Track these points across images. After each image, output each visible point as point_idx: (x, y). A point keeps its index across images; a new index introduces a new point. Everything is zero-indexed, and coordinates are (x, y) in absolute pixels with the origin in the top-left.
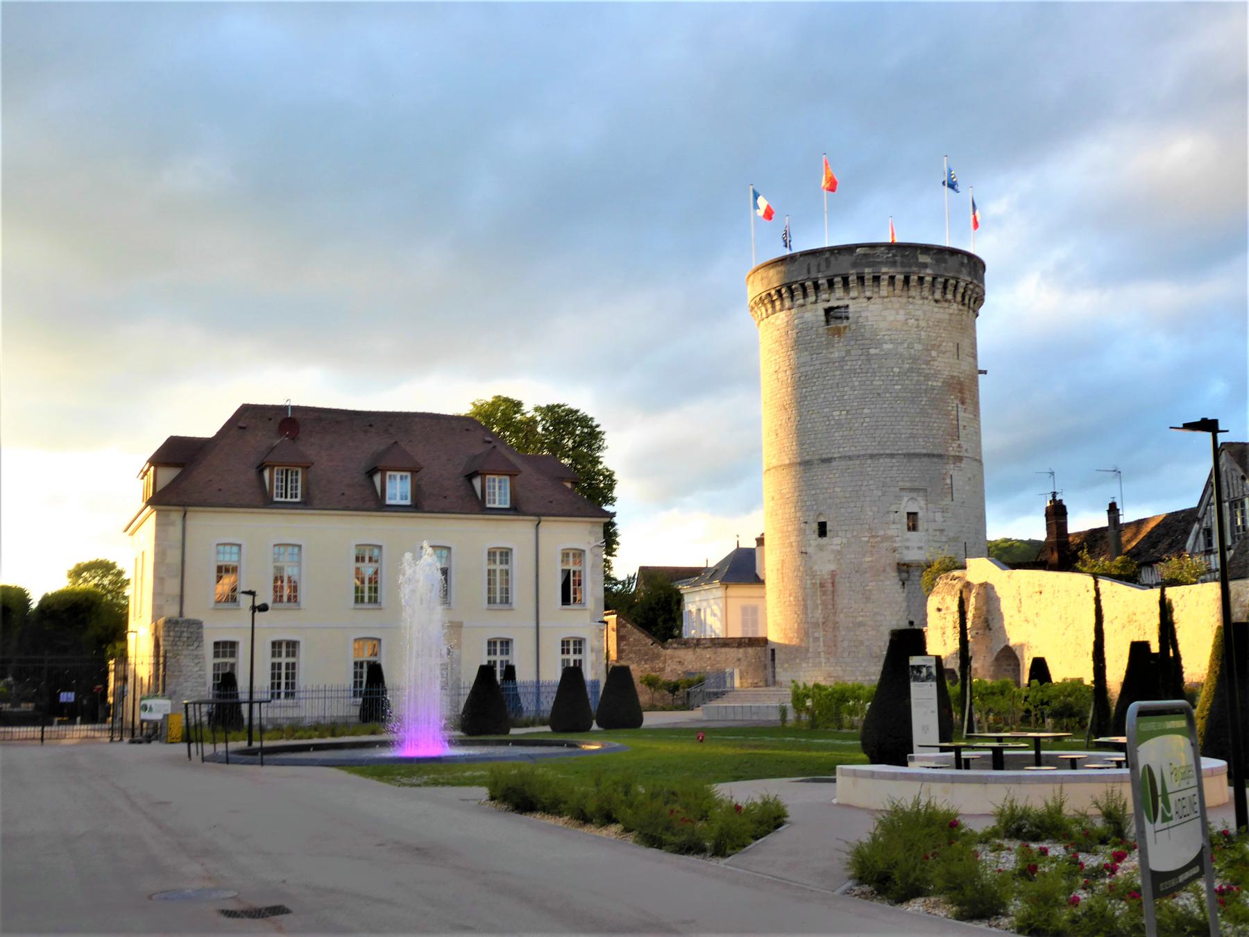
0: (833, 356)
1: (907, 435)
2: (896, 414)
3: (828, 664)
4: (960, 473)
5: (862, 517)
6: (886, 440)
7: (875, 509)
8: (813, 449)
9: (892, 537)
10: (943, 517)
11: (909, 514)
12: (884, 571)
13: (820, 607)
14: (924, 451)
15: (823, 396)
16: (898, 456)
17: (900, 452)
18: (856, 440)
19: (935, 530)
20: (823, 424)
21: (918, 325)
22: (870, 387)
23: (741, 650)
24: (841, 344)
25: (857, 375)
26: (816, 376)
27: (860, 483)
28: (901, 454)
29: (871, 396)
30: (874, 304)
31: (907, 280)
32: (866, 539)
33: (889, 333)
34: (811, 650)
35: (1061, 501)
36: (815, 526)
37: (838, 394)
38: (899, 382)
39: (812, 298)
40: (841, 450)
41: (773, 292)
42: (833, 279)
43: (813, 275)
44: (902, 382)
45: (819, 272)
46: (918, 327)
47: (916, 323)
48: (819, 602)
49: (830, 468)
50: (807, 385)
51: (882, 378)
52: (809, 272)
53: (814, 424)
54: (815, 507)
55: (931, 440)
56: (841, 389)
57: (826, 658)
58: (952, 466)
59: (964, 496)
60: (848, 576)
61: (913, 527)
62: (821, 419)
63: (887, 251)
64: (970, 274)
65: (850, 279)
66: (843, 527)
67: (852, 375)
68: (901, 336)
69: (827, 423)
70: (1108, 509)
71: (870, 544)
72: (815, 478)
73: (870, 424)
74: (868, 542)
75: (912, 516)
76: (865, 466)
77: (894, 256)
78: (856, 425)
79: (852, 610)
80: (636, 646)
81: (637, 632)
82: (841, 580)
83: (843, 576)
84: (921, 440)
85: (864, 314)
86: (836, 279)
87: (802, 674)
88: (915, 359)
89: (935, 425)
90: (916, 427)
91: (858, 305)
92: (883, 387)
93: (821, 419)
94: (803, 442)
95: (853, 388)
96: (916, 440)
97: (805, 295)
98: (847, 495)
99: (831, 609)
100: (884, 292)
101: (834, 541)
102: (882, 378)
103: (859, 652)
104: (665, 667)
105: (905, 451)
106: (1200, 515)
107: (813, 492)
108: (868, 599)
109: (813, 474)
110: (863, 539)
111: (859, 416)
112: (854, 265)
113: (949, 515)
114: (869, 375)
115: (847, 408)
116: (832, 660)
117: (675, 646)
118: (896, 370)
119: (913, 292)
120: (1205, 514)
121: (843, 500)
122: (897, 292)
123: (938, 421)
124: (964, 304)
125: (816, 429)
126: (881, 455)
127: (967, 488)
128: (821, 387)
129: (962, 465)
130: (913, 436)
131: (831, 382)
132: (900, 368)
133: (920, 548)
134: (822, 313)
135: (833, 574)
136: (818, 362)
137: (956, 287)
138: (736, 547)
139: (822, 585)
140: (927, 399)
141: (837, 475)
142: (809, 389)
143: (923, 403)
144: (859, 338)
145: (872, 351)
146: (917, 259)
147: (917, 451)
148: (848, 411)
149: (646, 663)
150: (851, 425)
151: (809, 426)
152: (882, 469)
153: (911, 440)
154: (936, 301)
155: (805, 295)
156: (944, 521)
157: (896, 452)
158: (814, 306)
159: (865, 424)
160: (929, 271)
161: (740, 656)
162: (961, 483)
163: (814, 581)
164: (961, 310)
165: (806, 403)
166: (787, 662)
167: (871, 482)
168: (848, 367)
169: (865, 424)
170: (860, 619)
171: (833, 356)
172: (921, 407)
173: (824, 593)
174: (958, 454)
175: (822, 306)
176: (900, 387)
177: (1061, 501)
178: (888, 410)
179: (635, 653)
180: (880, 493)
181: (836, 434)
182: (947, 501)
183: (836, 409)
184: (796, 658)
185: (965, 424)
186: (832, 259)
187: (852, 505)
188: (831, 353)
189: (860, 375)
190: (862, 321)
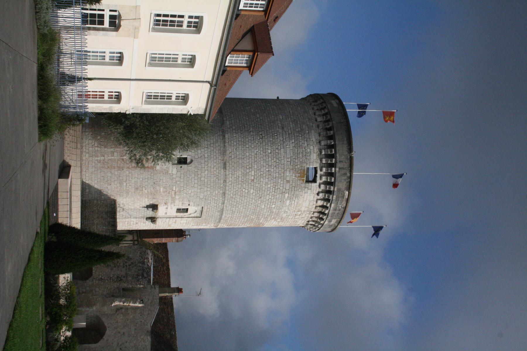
3: (96, 162)
5: (188, 187)
6: (233, 200)
7: (192, 194)
8: (233, 157)
9: (174, 202)
11: (187, 209)
15: (265, 165)
17: (225, 207)
22: (266, 193)
25: (274, 186)
28: (223, 208)
29: (260, 193)
30: (314, 197)
32: (174, 189)
34: (106, 149)
37: (264, 175)
40: (230, 176)
42: (334, 177)
43: (339, 165)
45: (340, 169)
50: (272, 153)
51: (270, 199)
52: (340, 162)
56: (267, 177)
61: (179, 210)
63: (343, 206)
67: (274, 184)
69: (248, 167)
70: (180, 287)
71: (171, 191)
72: (215, 157)
74: (173, 190)
76: (219, 190)
77: (339, 210)
78: (244, 185)
79: (131, 180)
83: (152, 175)
85: (309, 191)
92: (265, 200)
94: (238, 148)
98: (202, 179)
102: (270, 199)
105: (225, 209)
107: (206, 156)
108: (137, 189)
110: (174, 187)
111: (250, 187)
112: (339, 190)
114: (273, 193)
115: (255, 181)
118: (273, 206)
125: (245, 159)
126: (225, 198)
128: (270, 164)
132: (274, 208)
136: (285, 162)
141: (215, 172)
143: (252, 217)
144: (296, 189)
146: (333, 182)
147: (224, 214)
148: (253, 180)
151: (247, 154)
152: (216, 198)
154: (308, 221)
159: (244, 190)
165: (262, 153)
167: (209, 193)
168: (280, 181)
169: (244, 190)
170: (125, 184)
181: (240, 173)
183: (256, 174)
187: (196, 181)
188: (290, 172)
189: (274, 189)
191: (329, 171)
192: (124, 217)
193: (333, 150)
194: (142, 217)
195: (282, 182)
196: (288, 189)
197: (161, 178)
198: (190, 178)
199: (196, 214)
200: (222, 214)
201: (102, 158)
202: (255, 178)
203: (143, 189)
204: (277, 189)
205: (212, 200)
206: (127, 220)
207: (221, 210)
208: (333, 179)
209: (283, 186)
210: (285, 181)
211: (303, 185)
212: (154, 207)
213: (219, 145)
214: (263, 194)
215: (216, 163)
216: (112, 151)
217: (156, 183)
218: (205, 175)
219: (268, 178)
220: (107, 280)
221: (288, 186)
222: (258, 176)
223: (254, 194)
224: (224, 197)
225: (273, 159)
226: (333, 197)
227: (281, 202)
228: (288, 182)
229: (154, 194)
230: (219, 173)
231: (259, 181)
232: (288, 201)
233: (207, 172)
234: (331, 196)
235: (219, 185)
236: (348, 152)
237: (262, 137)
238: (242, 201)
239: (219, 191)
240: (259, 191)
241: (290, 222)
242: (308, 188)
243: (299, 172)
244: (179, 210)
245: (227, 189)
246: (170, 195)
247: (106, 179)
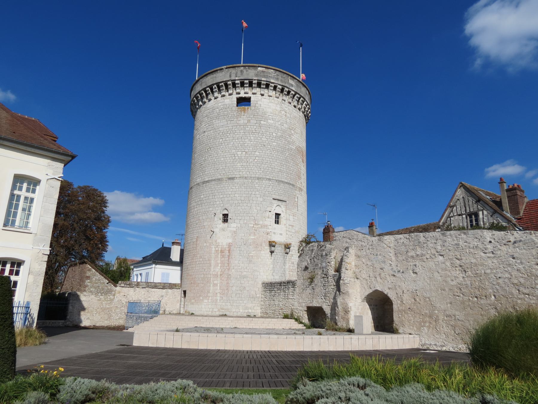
0: (240, 122)
1: (278, 170)
2: (273, 158)
5: (251, 212)
6: (267, 171)
7: (259, 208)
8: (224, 172)
9: (267, 226)
10: (293, 219)
12: (261, 245)
13: (219, 265)
14: (286, 181)
16: (273, 181)
18: (250, 169)
19: (289, 225)
20: (231, 158)
21: (286, 115)
22: (260, 141)
23: (164, 290)
24: (245, 116)
25: (253, 133)
26: (229, 132)
28: (275, 180)
29: (260, 145)
30: (265, 99)
32: (253, 225)
33: (272, 115)
37: (241, 143)
38: (276, 141)
40: (241, 173)
43: (233, 78)
44: (277, 142)
45: (236, 76)
47: (285, 114)
48: (219, 262)
49: (233, 183)
50: (223, 138)
51: (266, 137)
52: (230, 76)
53: (225, 159)
54: (222, 205)
55: (290, 176)
56: (243, 140)
57: (221, 297)
60: (239, 246)
61: (277, 222)
62: (230, 156)
66: (238, 218)
67: (250, 133)
68: (278, 118)
69: (234, 158)
71: (254, 229)
72: (223, 188)
73: (259, 160)
75: (277, 215)
76: (254, 183)
77: (278, 75)
78: (251, 160)
79: (240, 267)
80: (96, 283)
81: (99, 274)
83: (236, 246)
85: (259, 103)
87: (203, 307)
89: (292, 168)
90: (282, 167)
91: (256, 98)
92: (267, 142)
93: (230, 156)
94: (217, 168)
95: (250, 140)
96: (282, 173)
98: (243, 199)
99: (226, 266)
101: (232, 225)
102: (266, 137)
103: (242, 294)
104: (114, 298)
105: (276, 179)
107: (222, 196)
108: (250, 261)
112: (257, 75)
113: (296, 218)
116: (225, 298)
117: (123, 285)
118: (274, 134)
121: (240, 202)
125: (226, 161)
130: (280, 171)
133: (281, 234)
135: (230, 245)
136: (231, 125)
138: (161, 246)
139: (222, 252)
140: (288, 154)
141: (237, 187)
143: (287, 155)
145: (262, 122)
147: (283, 180)
149: (102, 295)
151: (222, 159)
152: (264, 186)
153: (280, 173)
156: (294, 221)
157: (272, 178)
161: (163, 294)
163: (217, 249)
165: (222, 147)
166: (194, 299)
167: (257, 193)
169: (256, 160)
170: (245, 273)
171: (240, 122)
172: (286, 157)
173: (223, 256)
175: (235, 97)
176: (276, 144)
178: (269, 155)
179: (95, 288)
180: (262, 200)
181: (239, 164)
182: (295, 211)
183: (240, 150)
184: (200, 296)
186: (245, 71)
187: (245, 205)
189: (255, 134)
190: (258, 106)
191: (239, 85)
192: (282, 275)
193: (220, 84)
194: (284, 258)
195: (249, 127)
196: (256, 121)
198: (241, 210)
199: (283, 206)
200: (283, 182)
201: (218, 295)
202: (244, 150)
203: (251, 256)
204: (256, 131)
205: (266, 190)
206: (287, 272)
207: (277, 182)
208: (246, 81)
209: (253, 126)
210: (248, 124)
211: (253, 108)
212: (272, 244)
213: (213, 185)
214: (261, 143)
215: (228, 187)
216: (213, 286)
217: (245, 243)
218: (239, 196)
219: (245, 139)
220: (325, 290)
221: (253, 121)
222: (242, 148)
223: (260, 151)
224: (262, 179)
225: (228, 136)
226: (264, 81)
227: (269, 128)
228: (249, 121)
229: (257, 245)
230: (237, 184)
231: (247, 147)
232: (269, 121)
233: (236, 195)
234: (263, 82)
235: (250, 183)
236: (222, 72)
237: (209, 148)
238: (267, 163)
239: (256, 183)
240: (257, 147)
241: (296, 122)
242: (255, 104)
243: (240, 112)
244: (277, 222)
245: (254, 176)
246: (258, 229)
247: (239, 292)
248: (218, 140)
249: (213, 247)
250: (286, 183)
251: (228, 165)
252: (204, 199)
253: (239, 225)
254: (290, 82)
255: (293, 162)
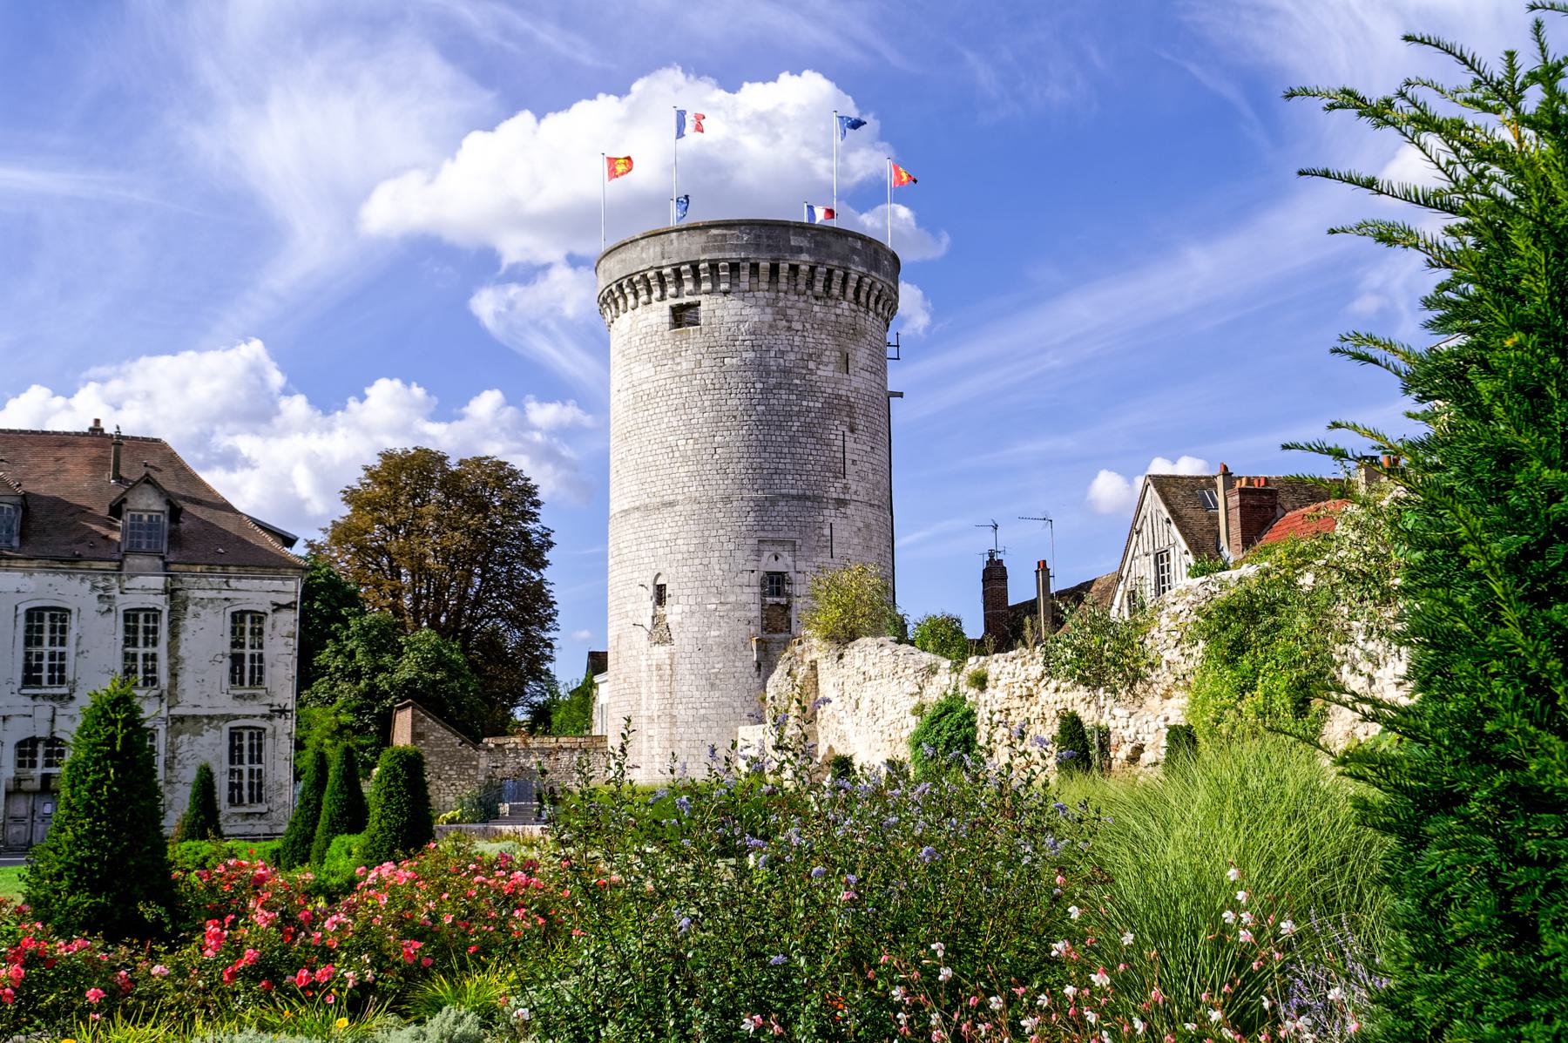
4: (845, 521)
8: (654, 490)
14: (794, 492)
15: (666, 420)
22: (724, 408)
26: (660, 394)
27: (706, 533)
29: (724, 419)
31: (774, 270)
35: (1000, 562)
36: (651, 588)
39: (657, 293)
41: (614, 287)
46: (789, 328)
48: (654, 689)
56: (688, 411)
58: (833, 512)
59: (850, 552)
64: (864, 264)
65: (702, 266)
74: (716, 610)
80: (439, 746)
82: (682, 661)
84: (788, 477)
86: (683, 268)
88: (786, 372)
97: (650, 292)
100: (745, 285)
106: (1124, 574)
107: (652, 545)
109: (652, 522)
114: (723, 391)
115: (696, 435)
118: (759, 385)
119: (783, 285)
120: (1129, 571)
122: (764, 286)
123: (814, 452)
124: (858, 303)
127: (856, 541)
128: (664, 409)
129: (848, 512)
131: (676, 402)
134: (667, 312)
137: (845, 280)
142: (651, 412)
143: (794, 429)
150: (699, 457)
151: (651, 459)
154: (817, 298)
155: (650, 292)
158: (660, 304)
159: (716, 457)
160: (805, 257)
162: (846, 534)
164: (854, 311)
167: (721, 532)
169: (716, 457)
170: (702, 711)
172: (791, 433)
174: (842, 496)
177: (1000, 562)
182: (823, 558)
185: (856, 457)
195: (698, 377)
197: (690, 636)
201: (657, 759)
208: (683, 268)
248: (641, 414)
249: (643, 657)
250: (793, 497)
251: (661, 472)
252: (625, 551)
253: (687, 609)
254: (792, 243)
255: (814, 441)
